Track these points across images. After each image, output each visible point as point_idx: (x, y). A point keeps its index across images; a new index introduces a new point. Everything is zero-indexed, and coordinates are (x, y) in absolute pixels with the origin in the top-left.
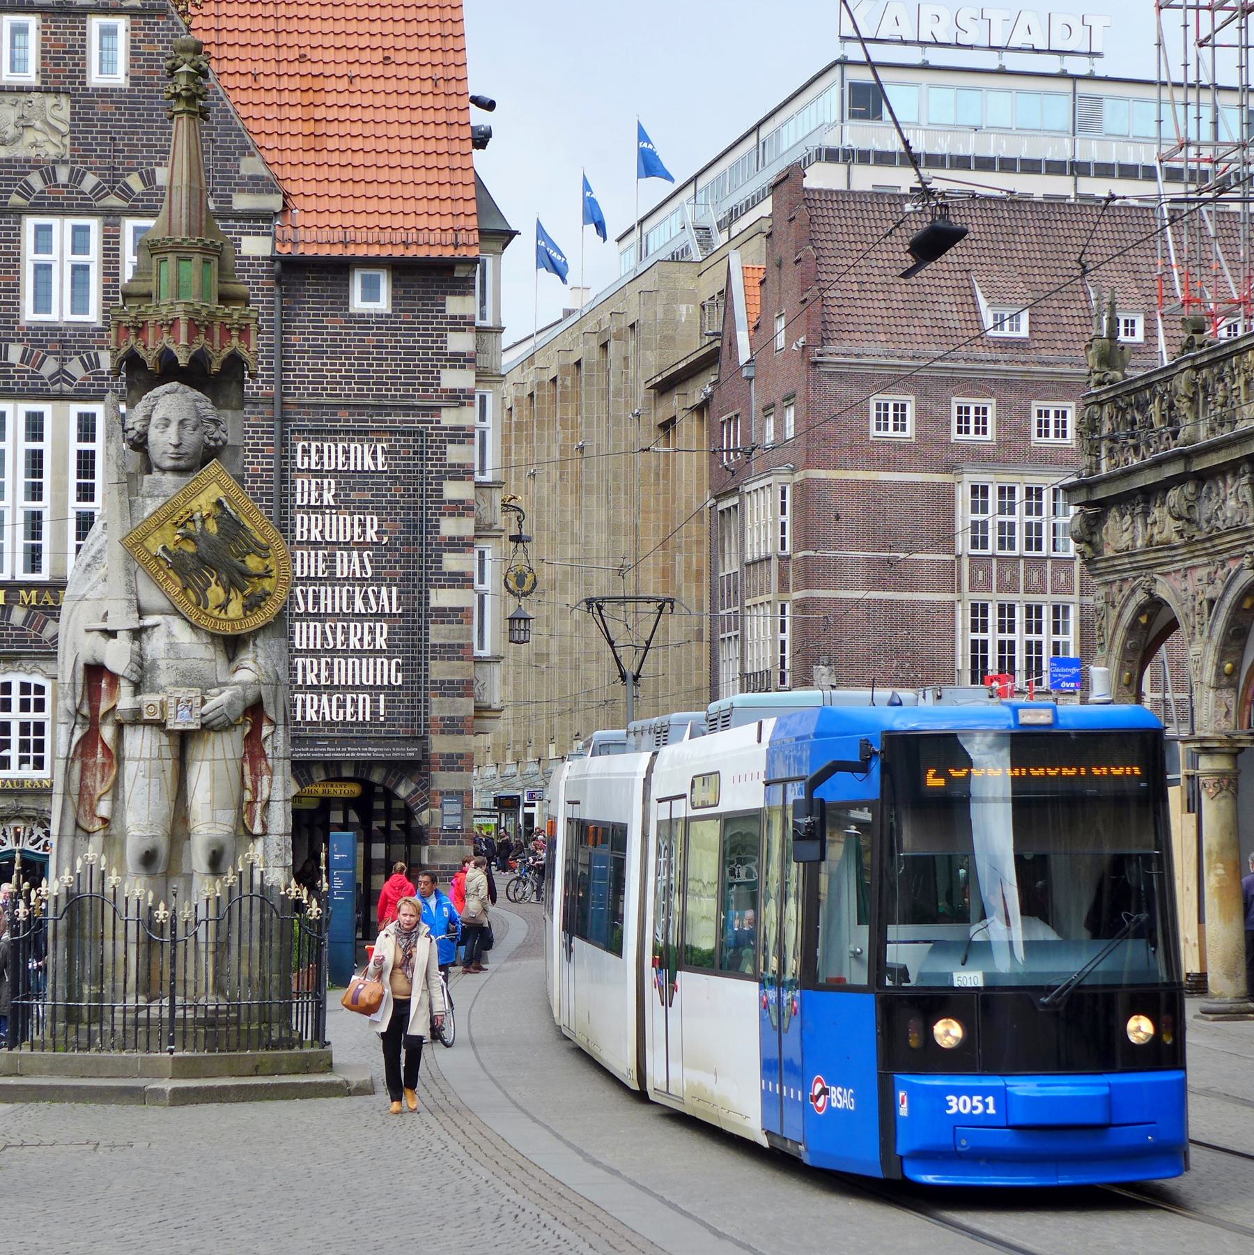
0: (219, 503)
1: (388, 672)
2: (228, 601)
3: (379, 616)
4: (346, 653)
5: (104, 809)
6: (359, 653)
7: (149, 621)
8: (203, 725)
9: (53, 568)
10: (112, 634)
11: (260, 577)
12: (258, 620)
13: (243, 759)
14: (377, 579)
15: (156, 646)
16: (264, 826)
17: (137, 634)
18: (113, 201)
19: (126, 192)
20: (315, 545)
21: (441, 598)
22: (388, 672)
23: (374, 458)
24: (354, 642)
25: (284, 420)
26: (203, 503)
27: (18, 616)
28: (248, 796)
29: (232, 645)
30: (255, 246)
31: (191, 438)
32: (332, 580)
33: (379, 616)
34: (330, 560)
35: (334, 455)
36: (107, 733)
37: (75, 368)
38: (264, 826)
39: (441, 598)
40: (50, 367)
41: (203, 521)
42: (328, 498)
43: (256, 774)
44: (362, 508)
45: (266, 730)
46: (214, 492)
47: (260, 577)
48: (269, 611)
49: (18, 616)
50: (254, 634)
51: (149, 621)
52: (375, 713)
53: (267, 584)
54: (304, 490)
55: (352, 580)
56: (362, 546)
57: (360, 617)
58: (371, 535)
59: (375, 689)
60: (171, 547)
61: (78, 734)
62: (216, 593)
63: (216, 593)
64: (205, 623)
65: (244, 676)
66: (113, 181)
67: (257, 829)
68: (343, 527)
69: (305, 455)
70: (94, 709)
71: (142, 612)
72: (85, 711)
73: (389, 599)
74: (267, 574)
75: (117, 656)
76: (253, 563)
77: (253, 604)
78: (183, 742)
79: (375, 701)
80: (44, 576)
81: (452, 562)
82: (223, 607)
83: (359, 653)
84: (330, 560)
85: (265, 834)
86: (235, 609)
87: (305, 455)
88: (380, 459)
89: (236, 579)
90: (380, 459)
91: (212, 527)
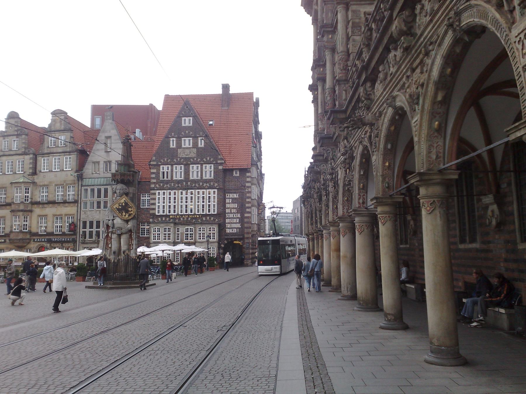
0: (125, 201)
1: (239, 226)
2: (126, 215)
3: (237, 218)
4: (233, 223)
5: (110, 246)
6: (235, 223)
7: (115, 218)
8: (121, 233)
9: (194, 212)
10: (110, 220)
11: (131, 211)
12: (130, 218)
13: (129, 238)
14: (237, 213)
15: (115, 221)
16: (132, 248)
17: (113, 220)
19: (204, 161)
20: (228, 208)
21: (246, 215)
22: (239, 226)
23: (237, 196)
24: (234, 221)
25: (225, 191)
26: (122, 201)
27: (189, 219)
28: (130, 244)
29: (127, 221)
30: (220, 167)
31: (122, 191)
32: (231, 213)
33: (237, 218)
34: (231, 210)
35: (231, 196)
36: (110, 235)
37: (197, 185)
38: (132, 248)
39: (246, 215)
40: (194, 185)
41: (122, 203)
42: (230, 202)
43: (131, 240)
44: (235, 203)
45: (132, 234)
46: (124, 199)
47: (131, 211)
48: (132, 216)
49: (189, 219)
50: (130, 219)
51: (115, 218)
52: (237, 231)
53: (132, 212)
54: (227, 201)
55: (234, 213)
56: (235, 208)
57: (235, 218)
58: (236, 207)
59: (237, 228)
60: (117, 207)
61: (106, 235)
62: (124, 214)
63: (124, 214)
64: (123, 218)
65: (129, 226)
66: (202, 160)
67: (131, 248)
68: (232, 206)
70: (108, 231)
71: (114, 217)
72: (106, 231)
73: (239, 216)
74: (132, 211)
75: (110, 223)
76: (130, 209)
77: (130, 215)
78: (119, 236)
79: (237, 230)
80: (193, 213)
81: (248, 210)
82: (125, 216)
83: (235, 223)
84: (231, 210)
85: (133, 249)
86: (127, 216)
88: (238, 196)
89: (127, 211)
90: (238, 196)
91: (124, 204)
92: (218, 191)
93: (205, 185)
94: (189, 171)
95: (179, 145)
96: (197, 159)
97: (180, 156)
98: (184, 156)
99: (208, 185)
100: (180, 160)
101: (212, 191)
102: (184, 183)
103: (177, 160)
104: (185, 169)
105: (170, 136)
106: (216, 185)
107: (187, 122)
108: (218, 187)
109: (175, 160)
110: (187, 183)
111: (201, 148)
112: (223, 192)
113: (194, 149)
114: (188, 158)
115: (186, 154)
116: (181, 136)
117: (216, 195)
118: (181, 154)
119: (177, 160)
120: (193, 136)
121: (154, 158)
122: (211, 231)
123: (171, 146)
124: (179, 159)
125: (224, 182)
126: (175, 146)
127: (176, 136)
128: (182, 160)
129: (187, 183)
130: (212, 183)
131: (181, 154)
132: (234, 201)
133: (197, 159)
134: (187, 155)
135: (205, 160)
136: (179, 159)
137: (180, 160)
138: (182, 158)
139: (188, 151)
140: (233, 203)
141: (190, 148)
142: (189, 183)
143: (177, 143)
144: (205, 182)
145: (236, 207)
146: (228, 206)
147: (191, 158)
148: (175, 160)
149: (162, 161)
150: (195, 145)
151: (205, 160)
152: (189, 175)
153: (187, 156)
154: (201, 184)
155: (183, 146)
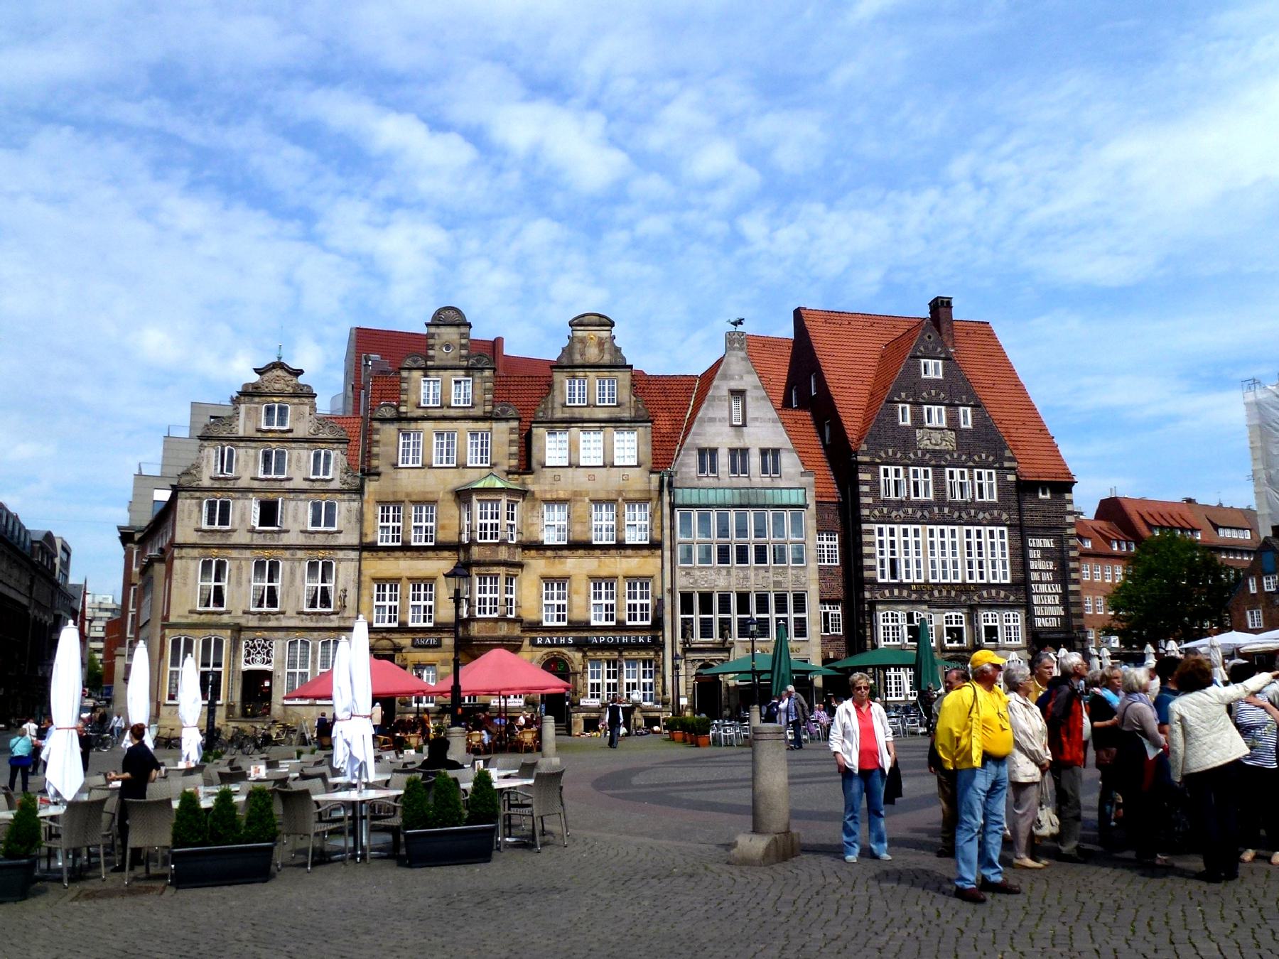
6: (1051, 605)
14: (1054, 582)
18: (971, 464)
19: (974, 461)
20: (1035, 570)
21: (1072, 587)
22: (1059, 611)
24: (1049, 602)
32: (1041, 582)
34: (1040, 575)
35: (1039, 543)
39: (1072, 587)
42: (1039, 556)
54: (1032, 554)
56: (1049, 571)
59: (1056, 616)
69: (1032, 542)
73: (1058, 589)
83: (1051, 605)
84: (1040, 575)
87: (1032, 542)
92: (1009, 531)
93: (981, 516)
94: (943, 480)
95: (918, 422)
96: (960, 456)
97: (921, 447)
98: (930, 447)
99: (987, 515)
100: (924, 455)
101: (997, 530)
102: (936, 509)
103: (916, 454)
104: (935, 478)
105: (896, 399)
106: (1005, 516)
107: (933, 370)
108: (1008, 523)
109: (912, 455)
110: (941, 510)
111: (966, 430)
112: (1021, 532)
113: (949, 433)
114: (940, 451)
115: (933, 441)
116: (921, 400)
117: (1006, 540)
118: (924, 441)
119: (916, 454)
120: (947, 402)
121: (864, 447)
122: (888, 621)
123: (901, 423)
124: (919, 453)
125: (1020, 511)
126: (908, 423)
127: (911, 400)
128: (928, 456)
129: (941, 510)
130: (996, 512)
131: (924, 441)
132: (1046, 554)
133: (960, 456)
134: (936, 445)
135: (976, 458)
136: (919, 453)
137: (924, 455)
138: (928, 451)
139: (937, 436)
140: (1044, 558)
141: (942, 429)
142: (946, 510)
143: (914, 416)
144: (980, 510)
145: (1051, 568)
146: (1033, 565)
147: (948, 452)
148: (912, 455)
149: (884, 456)
150: (953, 423)
151: (976, 458)
152: (944, 490)
153: (937, 448)
154: (973, 512)
155: (927, 424)
